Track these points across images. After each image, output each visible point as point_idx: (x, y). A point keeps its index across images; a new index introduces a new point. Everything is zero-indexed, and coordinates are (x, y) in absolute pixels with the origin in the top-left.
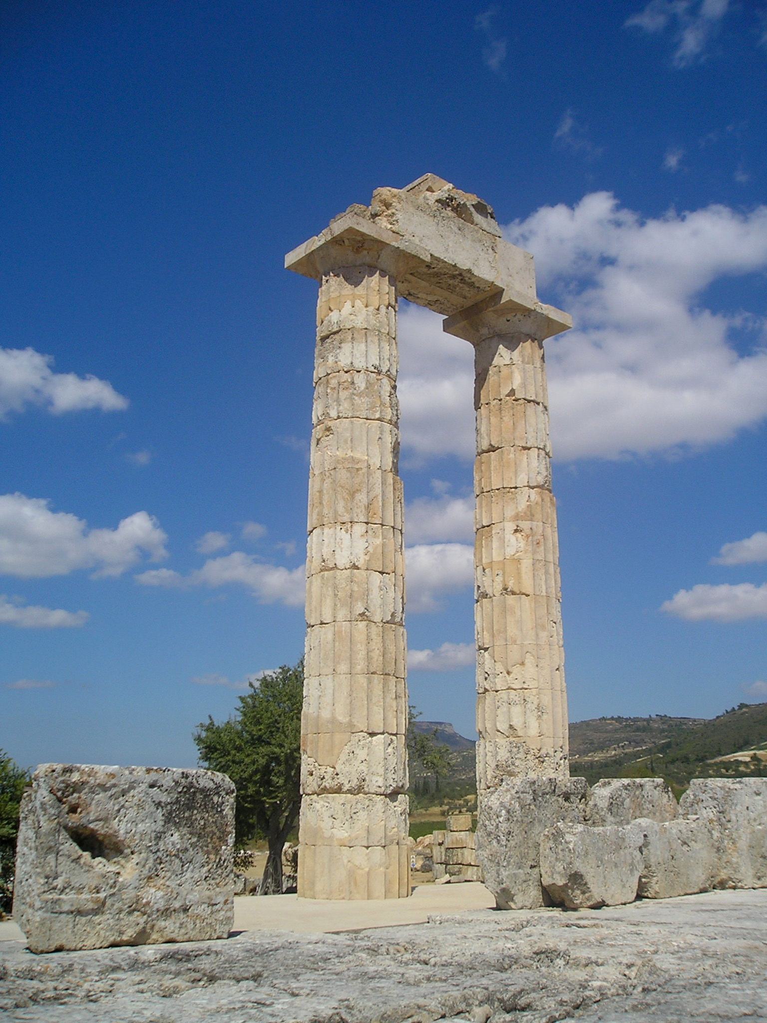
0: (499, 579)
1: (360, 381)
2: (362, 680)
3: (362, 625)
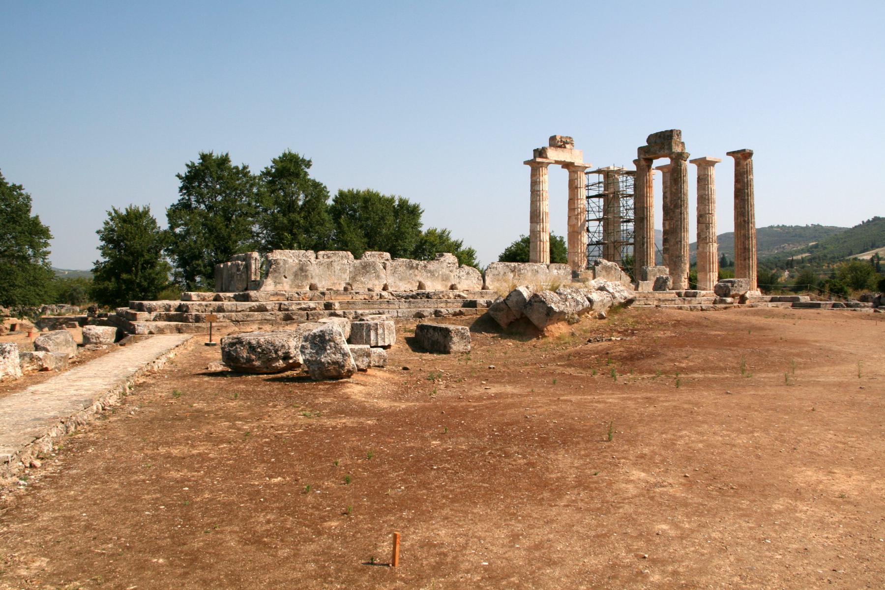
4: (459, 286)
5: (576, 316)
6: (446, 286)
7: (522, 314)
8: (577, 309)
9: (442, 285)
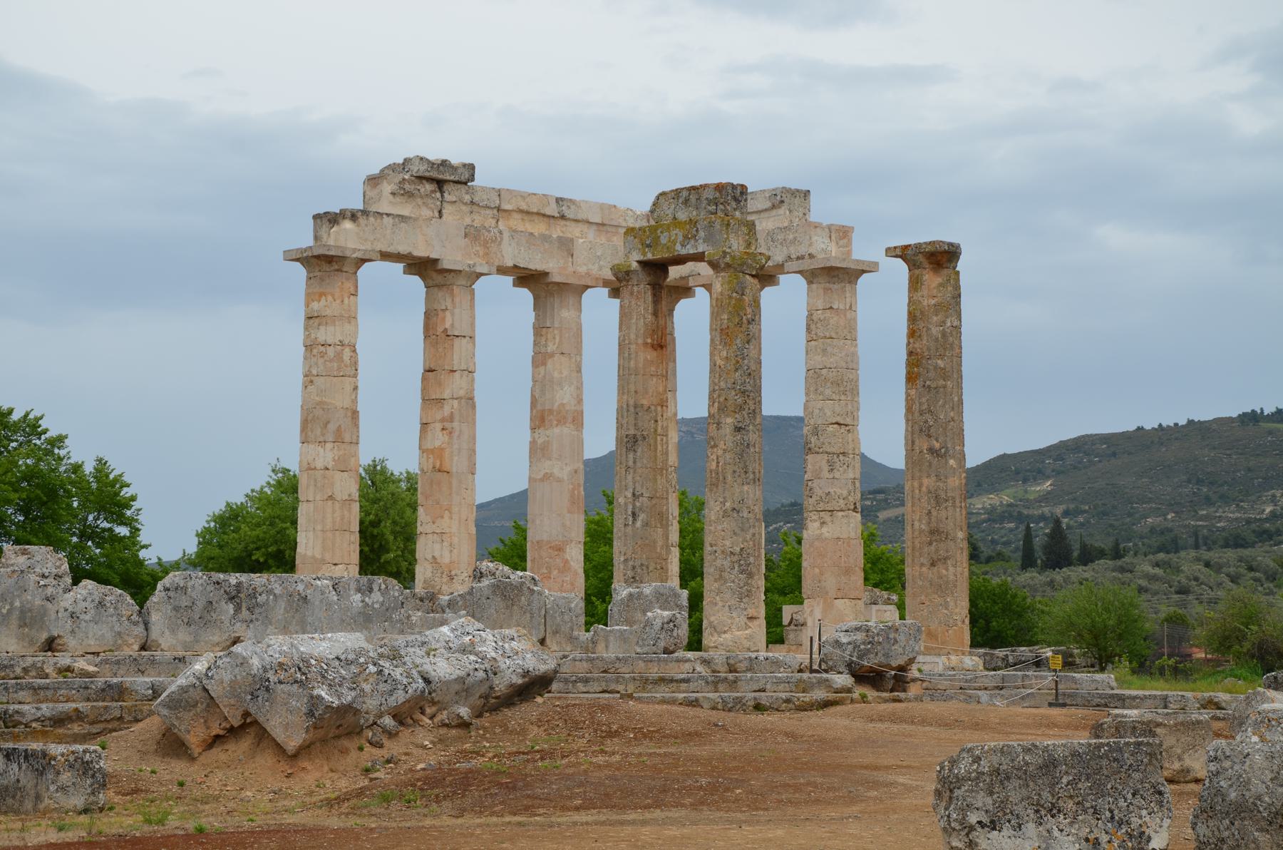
0: (431, 461)
2: (329, 534)
3: (330, 503)
4: (72, 642)
5: (388, 721)
6: (31, 642)
7: (247, 714)
8: (392, 701)
9: (21, 638)
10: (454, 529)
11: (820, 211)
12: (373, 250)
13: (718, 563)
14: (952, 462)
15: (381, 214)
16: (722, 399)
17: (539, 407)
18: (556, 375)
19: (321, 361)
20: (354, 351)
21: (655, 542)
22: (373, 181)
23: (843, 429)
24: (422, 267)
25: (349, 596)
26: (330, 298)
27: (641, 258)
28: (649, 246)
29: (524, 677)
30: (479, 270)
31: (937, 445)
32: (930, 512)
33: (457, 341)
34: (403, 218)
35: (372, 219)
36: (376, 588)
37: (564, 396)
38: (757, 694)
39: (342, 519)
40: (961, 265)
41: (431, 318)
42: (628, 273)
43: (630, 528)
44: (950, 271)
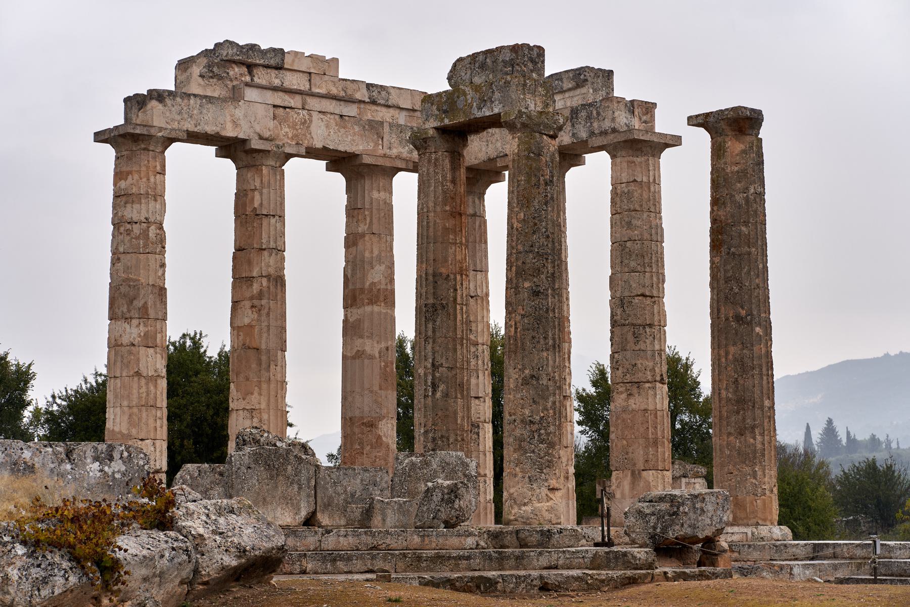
0: (241, 338)
1: (136, 229)
2: (135, 410)
3: (136, 379)
10: (263, 406)
11: (622, 89)
12: (179, 130)
13: (518, 432)
14: (758, 329)
15: (189, 95)
16: (520, 263)
17: (351, 287)
18: (367, 254)
19: (129, 238)
20: (161, 228)
21: (455, 413)
22: (183, 65)
23: (648, 301)
24: (228, 147)
25: (85, 464)
26: (136, 177)
27: (437, 124)
28: (445, 112)
29: (239, 557)
30: (288, 150)
31: (743, 313)
32: (736, 380)
33: (265, 222)
34: (210, 99)
35: (178, 99)
36: (116, 455)
37: (376, 275)
38: (545, 573)
39: (148, 395)
40: (763, 134)
41: (242, 198)
42: (425, 140)
43: (430, 399)
44: (754, 138)
